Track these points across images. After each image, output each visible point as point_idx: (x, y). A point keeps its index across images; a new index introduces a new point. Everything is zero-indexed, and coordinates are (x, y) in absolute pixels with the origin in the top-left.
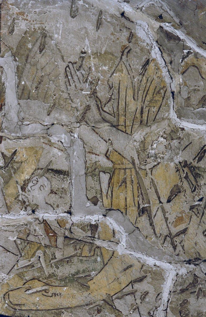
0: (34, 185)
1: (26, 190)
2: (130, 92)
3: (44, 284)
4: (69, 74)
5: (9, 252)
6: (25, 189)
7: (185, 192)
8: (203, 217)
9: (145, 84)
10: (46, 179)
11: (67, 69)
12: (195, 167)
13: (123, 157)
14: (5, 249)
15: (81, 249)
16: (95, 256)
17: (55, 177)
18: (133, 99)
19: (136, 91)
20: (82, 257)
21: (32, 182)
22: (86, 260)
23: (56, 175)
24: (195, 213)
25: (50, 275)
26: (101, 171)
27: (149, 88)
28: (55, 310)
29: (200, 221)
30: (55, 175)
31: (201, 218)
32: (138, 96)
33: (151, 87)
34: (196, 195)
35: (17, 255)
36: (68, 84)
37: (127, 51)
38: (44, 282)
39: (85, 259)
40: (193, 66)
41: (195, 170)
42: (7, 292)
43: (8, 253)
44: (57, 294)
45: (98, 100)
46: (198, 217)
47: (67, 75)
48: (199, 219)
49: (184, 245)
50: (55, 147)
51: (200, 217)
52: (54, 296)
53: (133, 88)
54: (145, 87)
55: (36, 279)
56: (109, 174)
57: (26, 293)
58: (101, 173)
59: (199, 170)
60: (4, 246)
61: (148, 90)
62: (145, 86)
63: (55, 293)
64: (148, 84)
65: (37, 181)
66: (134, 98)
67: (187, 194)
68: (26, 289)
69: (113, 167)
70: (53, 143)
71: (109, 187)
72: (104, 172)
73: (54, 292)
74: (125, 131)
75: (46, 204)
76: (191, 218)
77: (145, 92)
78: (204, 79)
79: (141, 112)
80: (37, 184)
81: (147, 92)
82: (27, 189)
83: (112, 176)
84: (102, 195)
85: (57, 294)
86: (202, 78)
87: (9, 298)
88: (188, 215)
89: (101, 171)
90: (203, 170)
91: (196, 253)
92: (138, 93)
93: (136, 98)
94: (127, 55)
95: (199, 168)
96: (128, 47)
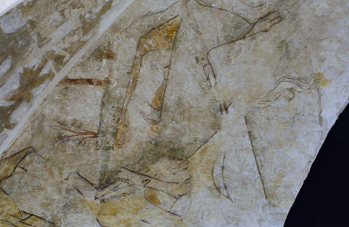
7: (125, 193)
12: (100, 183)
24: (146, 184)
31: (152, 178)
34: (128, 183)
41: (103, 184)
46: (150, 181)
48: (152, 180)
49: (179, 195)
51: (150, 179)
59: (103, 180)
67: (127, 192)
76: (152, 188)
78: (12, 174)
86: (11, 176)
88: (148, 191)
90: (103, 176)
91: (186, 183)
95: (101, 180)
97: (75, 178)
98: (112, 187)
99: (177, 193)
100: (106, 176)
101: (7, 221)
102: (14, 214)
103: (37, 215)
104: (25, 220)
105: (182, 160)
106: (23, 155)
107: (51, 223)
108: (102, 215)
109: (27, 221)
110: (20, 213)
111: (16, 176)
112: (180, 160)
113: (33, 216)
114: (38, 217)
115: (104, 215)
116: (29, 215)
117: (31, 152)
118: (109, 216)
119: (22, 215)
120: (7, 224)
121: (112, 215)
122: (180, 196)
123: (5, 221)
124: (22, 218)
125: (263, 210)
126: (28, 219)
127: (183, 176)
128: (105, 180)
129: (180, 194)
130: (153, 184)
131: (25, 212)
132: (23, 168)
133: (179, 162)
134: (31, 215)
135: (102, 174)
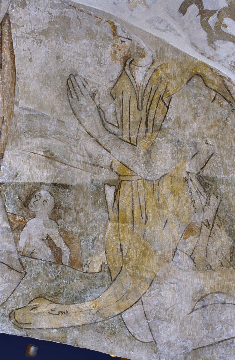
0: (36, 201)
1: (29, 206)
2: (134, 103)
3: (50, 302)
4: (70, 85)
5: (13, 269)
6: (28, 204)
7: (194, 203)
8: (214, 228)
9: (149, 94)
10: (49, 194)
11: (69, 81)
12: (204, 176)
13: (128, 168)
14: (9, 266)
15: (87, 265)
16: (102, 273)
17: (58, 191)
18: (137, 109)
19: (140, 99)
20: (89, 273)
21: (35, 198)
22: (93, 277)
23: (59, 190)
24: (205, 224)
25: (56, 293)
26: (106, 184)
27: (153, 97)
28: (63, 329)
29: (211, 232)
30: (58, 190)
32: (142, 106)
33: (155, 96)
34: (206, 205)
35: (22, 273)
36: (70, 96)
37: (129, 62)
38: (50, 300)
39: (91, 275)
40: (197, 75)
42: (13, 311)
43: (12, 271)
44: (64, 312)
45: (100, 111)
46: (208, 228)
47: (69, 87)
48: (209, 231)
49: (194, 258)
50: (58, 161)
51: (210, 228)
52: (60, 315)
53: (137, 98)
54: (149, 97)
55: (42, 297)
56: (114, 187)
57: (32, 311)
58: (106, 186)
60: (9, 264)
61: (152, 100)
62: (149, 95)
63: (62, 311)
64: (152, 94)
65: (39, 196)
66: (138, 108)
68: (32, 308)
69: (119, 179)
70: (56, 157)
71: (115, 200)
72: (110, 185)
73: (61, 310)
74: (129, 142)
75: (50, 220)
77: (150, 102)
78: (208, 87)
79: (146, 122)
80: (40, 199)
81: (151, 102)
82: (29, 204)
83: (117, 188)
84: (108, 208)
85: (64, 312)
86: (207, 86)
87: (14, 317)
89: (106, 184)
90: (212, 180)
91: (207, 266)
92: (142, 102)
93: (140, 107)
94: (130, 65)
95: (207, 177)
96: (130, 58)
97: (208, 151)
98: (201, 189)
99: (196, 256)
100: (211, 182)
101: (160, 82)
102: (168, 90)
103: (168, 113)
104: (163, 100)
105: (231, 260)
106: (228, 98)
107: (161, 128)
108: (171, 179)
109: (161, 104)
110: (170, 96)
111: (207, 91)
112: (230, 258)
113: (166, 109)
114: (166, 114)
115: (171, 182)
116: (167, 105)
117: (231, 106)
118: (170, 186)
119: (167, 97)
120: (157, 83)
121: (171, 189)
122: (193, 260)
123: (160, 80)
124: (164, 98)
125: (181, 347)
126: (163, 104)
127: (215, 262)
128: (207, 182)
129: (195, 259)
130: (205, 231)
131: (170, 101)
132: (215, 98)
133: (229, 258)
134: (168, 107)
135: (213, 178)
